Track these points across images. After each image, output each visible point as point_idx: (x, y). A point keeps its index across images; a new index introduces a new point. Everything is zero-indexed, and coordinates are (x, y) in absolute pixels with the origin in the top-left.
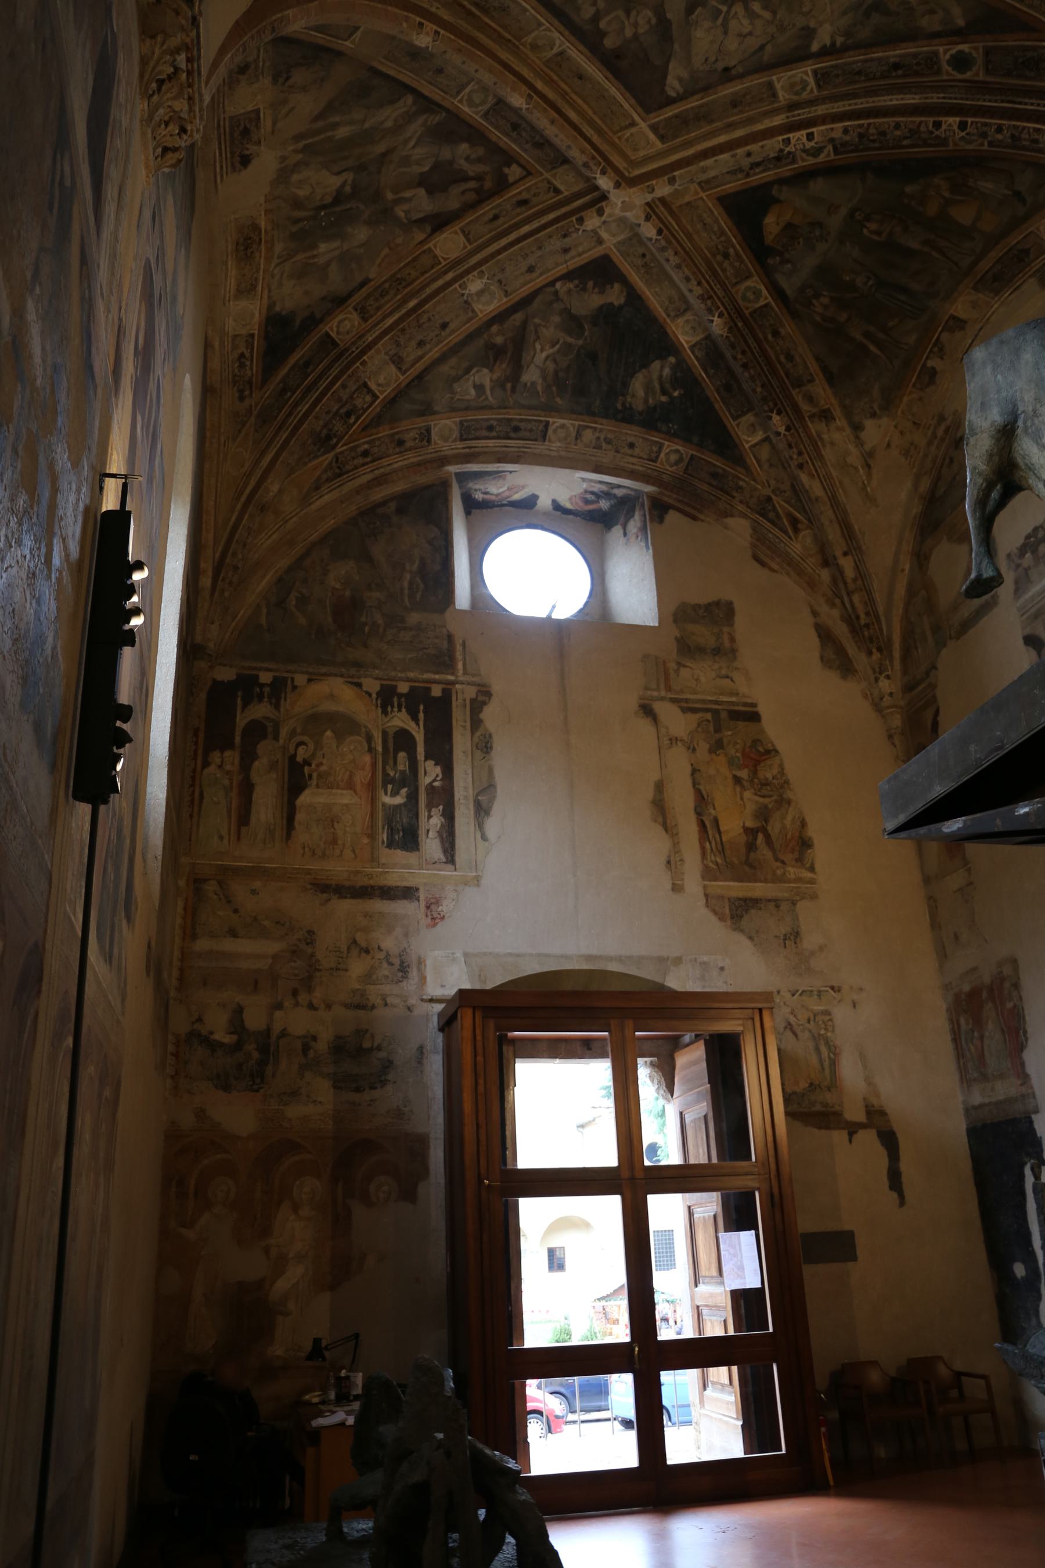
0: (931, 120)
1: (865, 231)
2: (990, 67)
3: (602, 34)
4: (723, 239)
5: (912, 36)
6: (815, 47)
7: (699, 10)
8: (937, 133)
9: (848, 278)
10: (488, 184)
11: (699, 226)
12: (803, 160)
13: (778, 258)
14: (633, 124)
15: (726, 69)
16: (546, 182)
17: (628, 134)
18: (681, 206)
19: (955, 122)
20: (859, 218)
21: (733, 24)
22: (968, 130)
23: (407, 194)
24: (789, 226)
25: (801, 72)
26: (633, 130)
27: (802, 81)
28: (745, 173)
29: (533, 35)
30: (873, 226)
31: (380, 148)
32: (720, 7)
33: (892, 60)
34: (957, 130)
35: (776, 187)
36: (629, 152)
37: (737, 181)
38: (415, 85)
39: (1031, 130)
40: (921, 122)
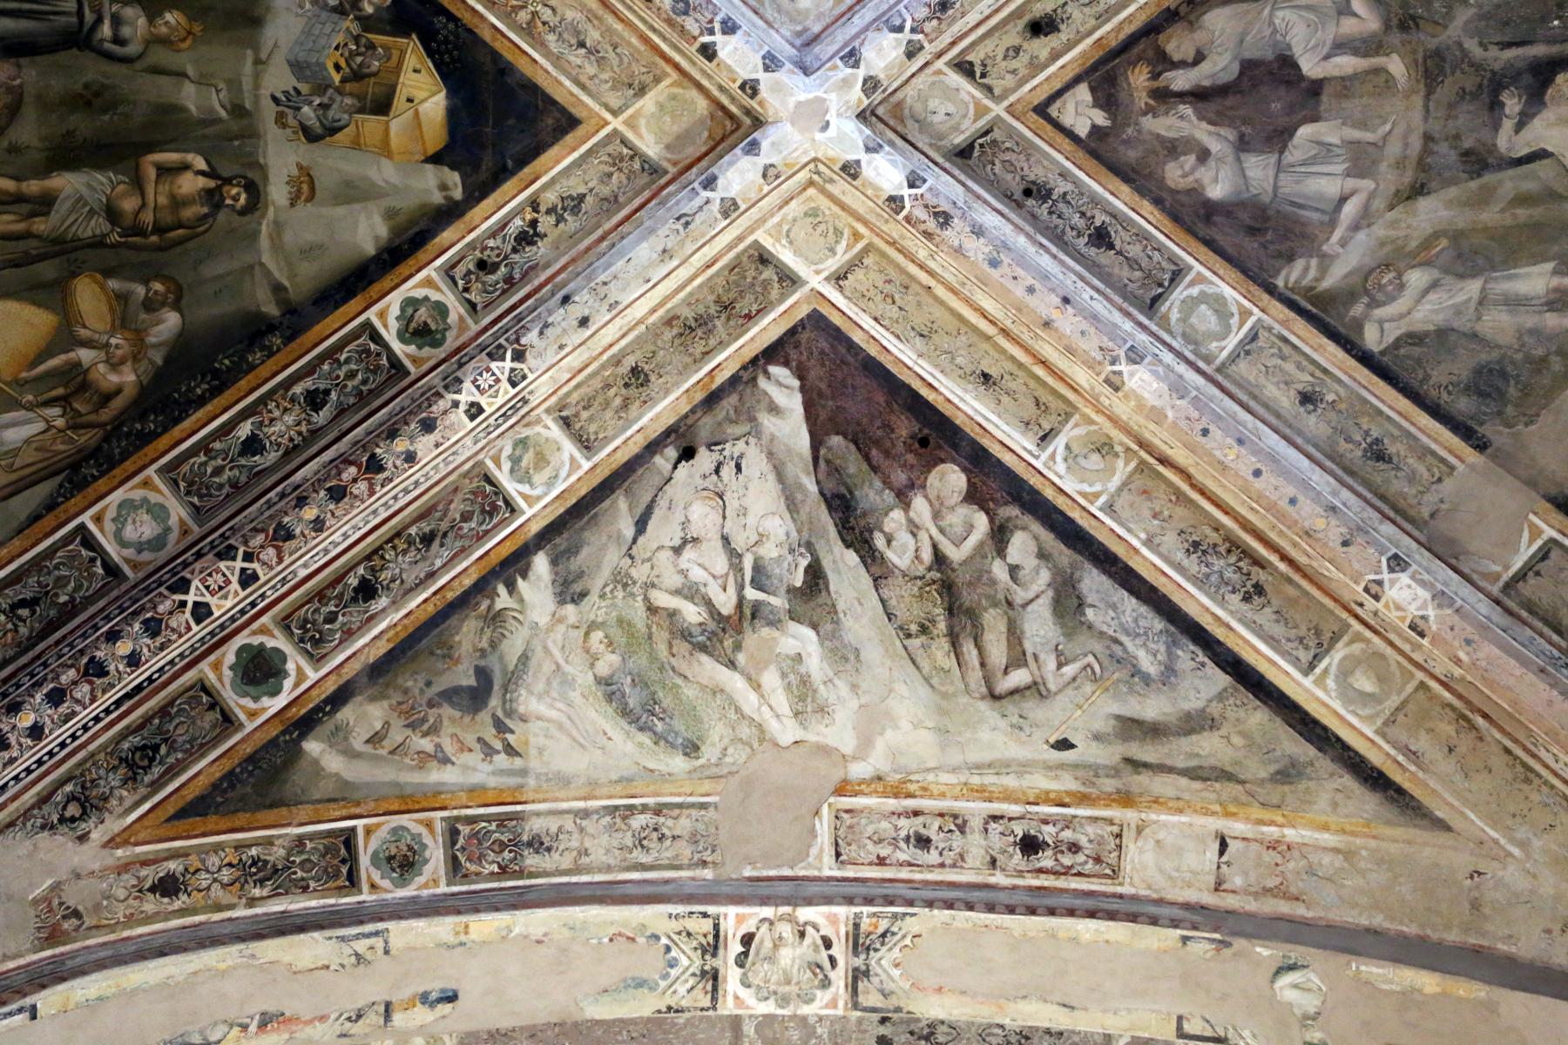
1: (200, 164)
2: (205, 699)
3: (973, 496)
4: (523, 16)
5: (381, 671)
6: (541, 563)
7: (798, 582)
8: (239, 564)
9: (169, 17)
10: (1139, 79)
11: (593, 36)
12: (428, 282)
13: (370, 10)
14: (839, 278)
15: (688, 454)
16: (997, 91)
17: (840, 248)
18: (657, 80)
19: (219, 607)
20: (234, 191)
21: (721, 564)
22: (188, 615)
23: (1346, 64)
24: (382, 106)
25: (539, 498)
26: (833, 264)
27: (525, 478)
28: (543, 208)
29: (1116, 482)
30: (190, 184)
31: (1430, 213)
32: (760, 596)
33: (383, 601)
34: (208, 598)
35: (458, 194)
36: (824, 203)
37: (553, 181)
38: (1363, 374)
39: (78, 708)
40: (280, 560)
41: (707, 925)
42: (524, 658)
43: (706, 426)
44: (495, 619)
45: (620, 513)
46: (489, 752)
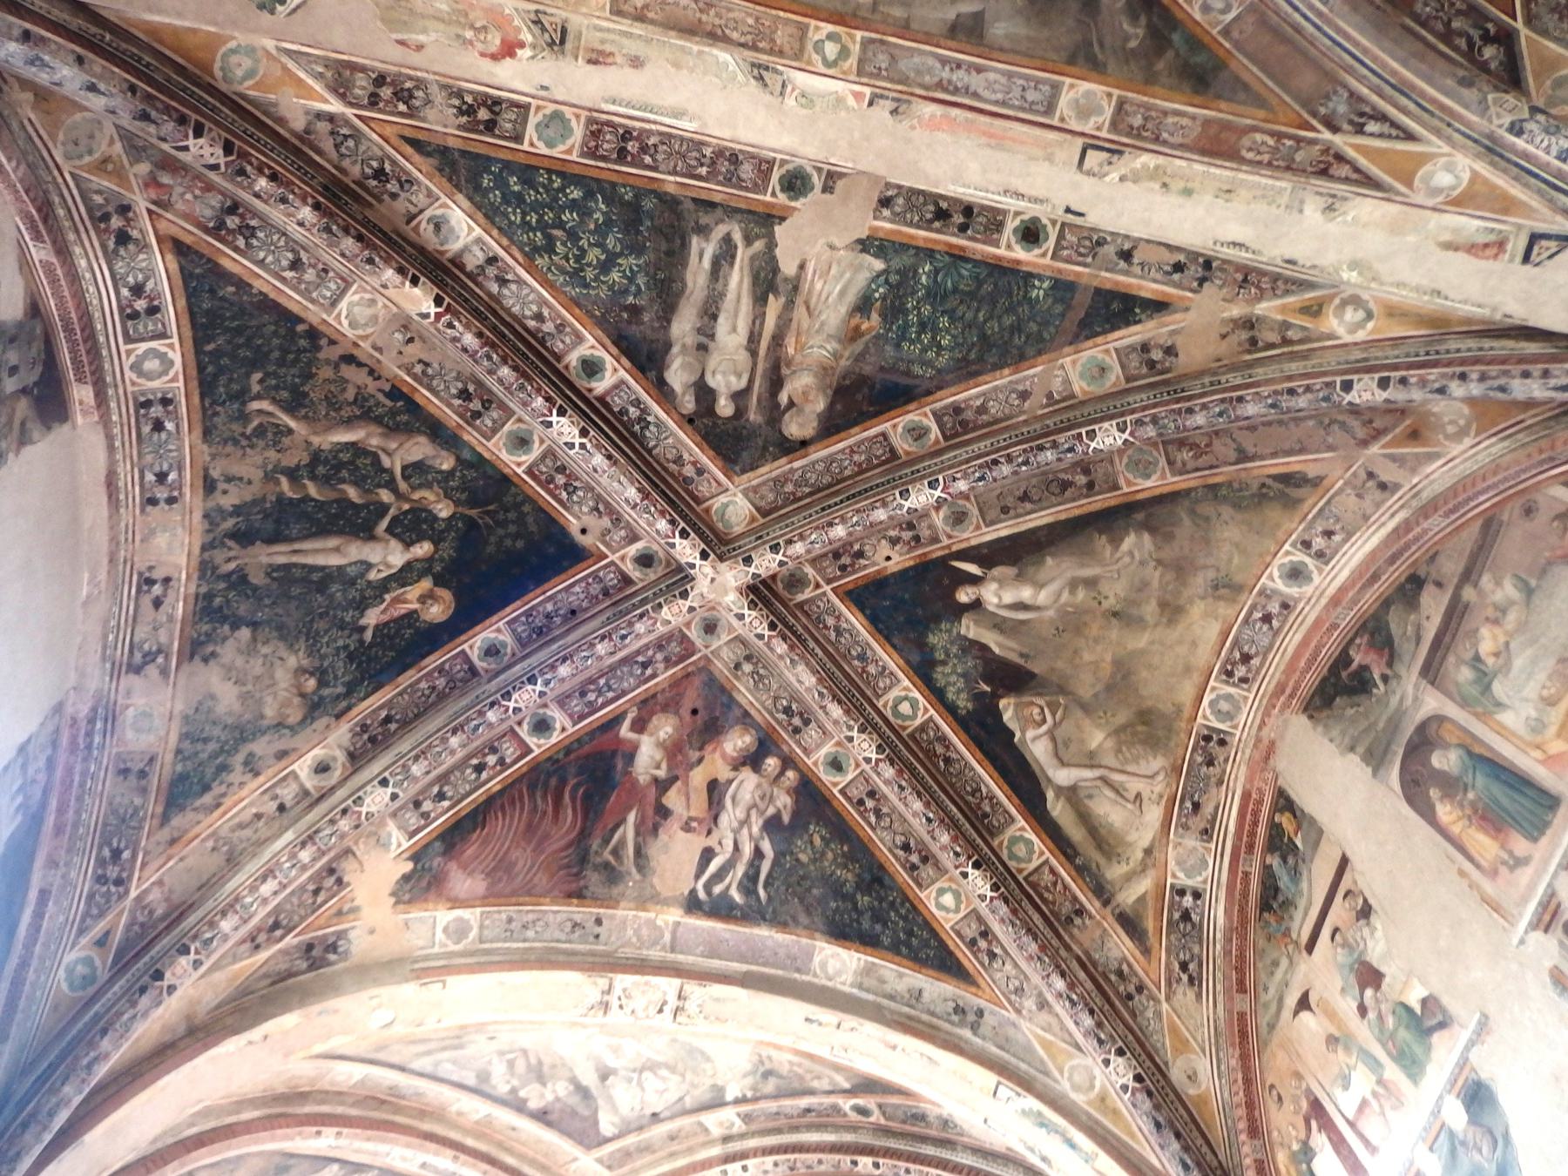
0: (848, 1159)
3: (525, 1101)
41: (679, 1019)
42: (745, 1076)
43: (645, 1121)
44: (754, 1089)
45: (689, 1102)
46: (770, 1058)
